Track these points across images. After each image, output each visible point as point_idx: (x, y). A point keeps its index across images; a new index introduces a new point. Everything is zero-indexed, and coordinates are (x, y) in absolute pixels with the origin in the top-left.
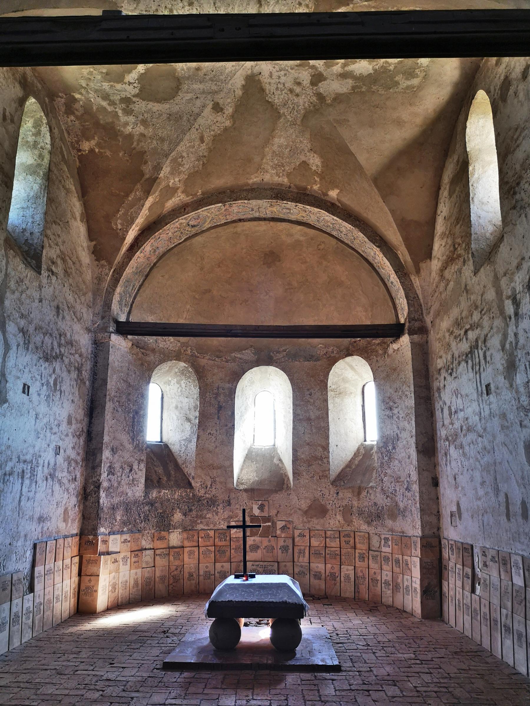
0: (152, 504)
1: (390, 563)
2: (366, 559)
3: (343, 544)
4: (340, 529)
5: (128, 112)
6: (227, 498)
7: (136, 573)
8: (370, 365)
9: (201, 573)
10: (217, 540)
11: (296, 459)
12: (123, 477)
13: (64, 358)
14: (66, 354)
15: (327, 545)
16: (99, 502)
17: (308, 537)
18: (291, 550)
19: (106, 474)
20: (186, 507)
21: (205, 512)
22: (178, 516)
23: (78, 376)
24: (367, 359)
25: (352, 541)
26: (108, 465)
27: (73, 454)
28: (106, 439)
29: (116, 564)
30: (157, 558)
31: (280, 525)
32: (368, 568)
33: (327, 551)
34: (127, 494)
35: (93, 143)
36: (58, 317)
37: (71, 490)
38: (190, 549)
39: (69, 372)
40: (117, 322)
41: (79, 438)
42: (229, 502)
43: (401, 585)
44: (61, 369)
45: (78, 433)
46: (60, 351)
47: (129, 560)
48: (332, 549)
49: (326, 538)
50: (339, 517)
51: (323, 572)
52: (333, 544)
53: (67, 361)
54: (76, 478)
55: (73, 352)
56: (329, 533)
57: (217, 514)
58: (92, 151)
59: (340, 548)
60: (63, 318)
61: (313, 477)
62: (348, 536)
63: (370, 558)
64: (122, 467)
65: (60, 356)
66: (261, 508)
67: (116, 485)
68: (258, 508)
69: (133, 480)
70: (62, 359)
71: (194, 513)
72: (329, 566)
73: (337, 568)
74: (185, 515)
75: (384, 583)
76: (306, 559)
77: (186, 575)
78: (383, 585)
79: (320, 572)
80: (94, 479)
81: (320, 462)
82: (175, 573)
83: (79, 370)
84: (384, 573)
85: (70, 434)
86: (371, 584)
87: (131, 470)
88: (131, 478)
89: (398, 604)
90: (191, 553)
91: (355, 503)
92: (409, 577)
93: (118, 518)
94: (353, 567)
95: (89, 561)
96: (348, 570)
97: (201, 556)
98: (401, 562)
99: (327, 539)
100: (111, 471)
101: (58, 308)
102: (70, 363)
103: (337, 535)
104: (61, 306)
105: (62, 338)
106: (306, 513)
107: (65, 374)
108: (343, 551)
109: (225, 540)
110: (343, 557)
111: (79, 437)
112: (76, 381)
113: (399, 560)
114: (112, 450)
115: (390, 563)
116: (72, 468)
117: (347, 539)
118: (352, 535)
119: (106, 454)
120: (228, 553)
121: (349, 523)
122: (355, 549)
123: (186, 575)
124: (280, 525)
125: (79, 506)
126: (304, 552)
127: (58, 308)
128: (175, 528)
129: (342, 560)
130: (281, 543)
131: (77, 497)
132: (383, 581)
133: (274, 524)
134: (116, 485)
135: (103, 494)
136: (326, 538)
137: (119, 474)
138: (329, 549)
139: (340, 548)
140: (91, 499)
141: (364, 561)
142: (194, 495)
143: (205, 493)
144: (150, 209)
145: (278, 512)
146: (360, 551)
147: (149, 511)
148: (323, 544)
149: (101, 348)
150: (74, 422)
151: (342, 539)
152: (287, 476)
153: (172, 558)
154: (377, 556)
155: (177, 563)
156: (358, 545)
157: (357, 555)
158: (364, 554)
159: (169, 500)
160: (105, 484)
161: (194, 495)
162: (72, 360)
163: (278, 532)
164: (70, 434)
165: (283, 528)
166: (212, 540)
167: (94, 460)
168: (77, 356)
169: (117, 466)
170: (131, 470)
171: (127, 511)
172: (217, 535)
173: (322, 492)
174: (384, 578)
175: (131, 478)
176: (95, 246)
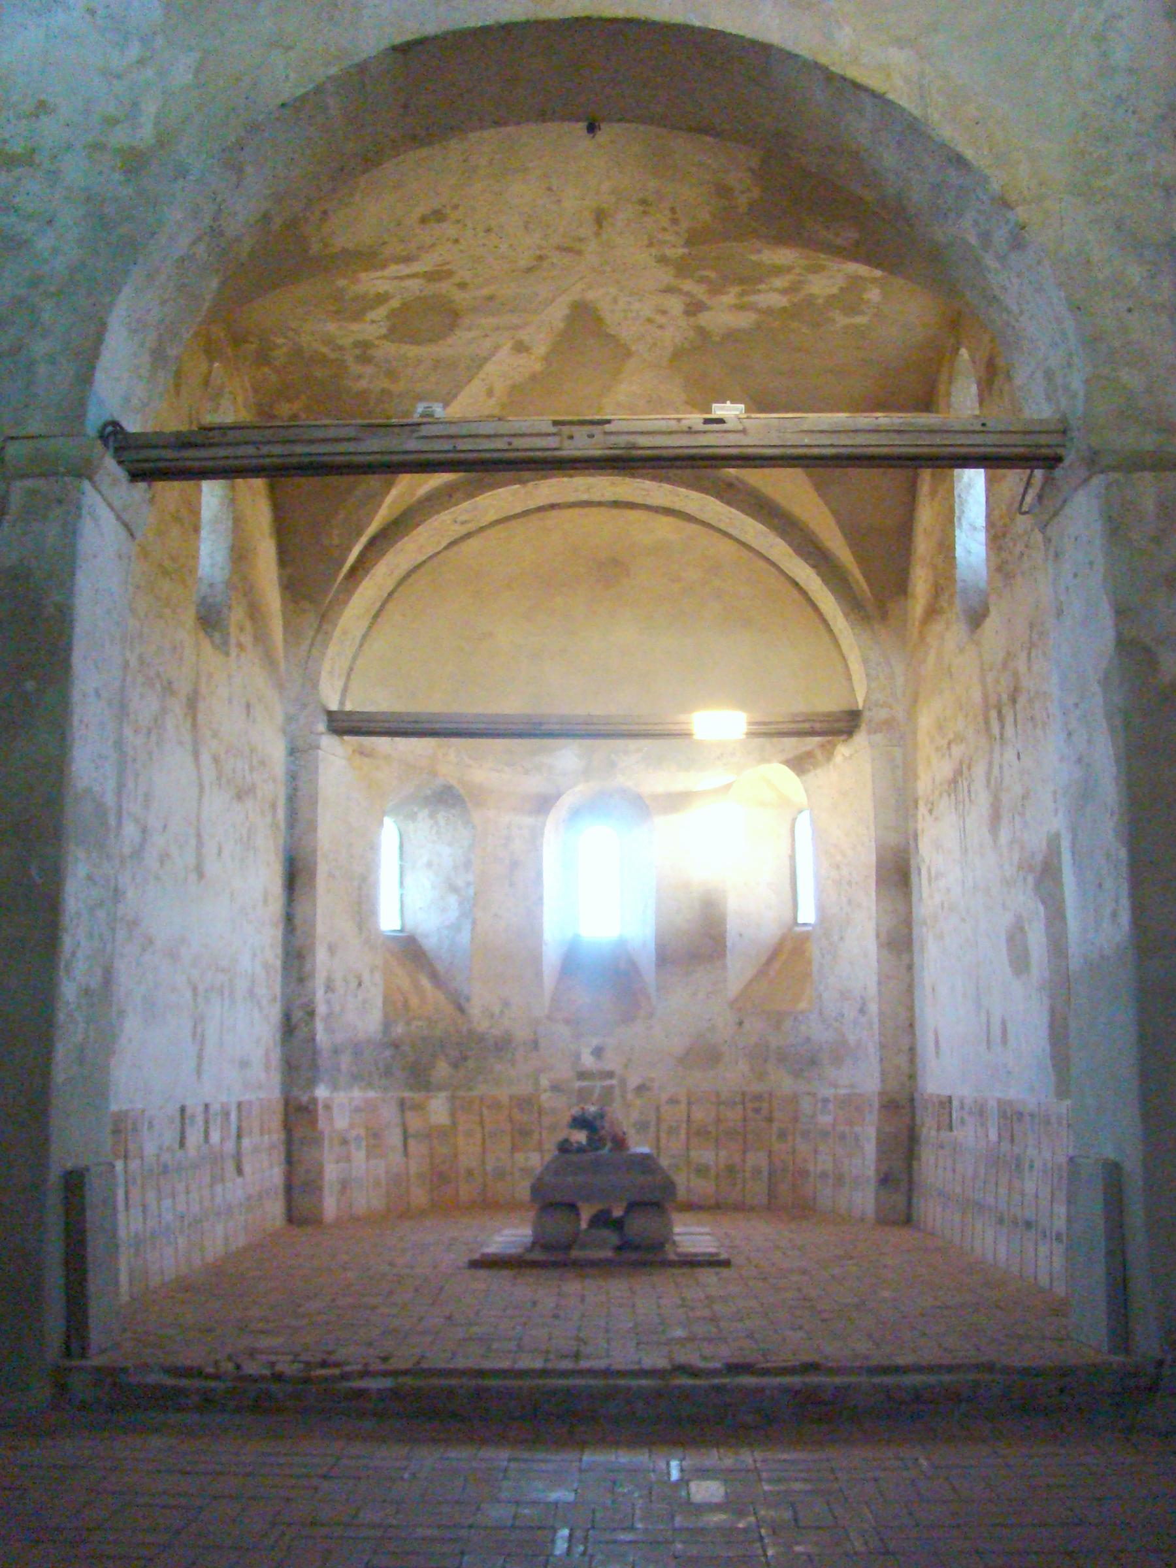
0: (396, 1046)
9: (489, 1168)
18: (652, 1129)
22: (442, 1069)
25: (765, 1105)
30: (411, 1141)
40: (330, 714)
64: (345, 980)
68: (592, 1053)
71: (471, 1064)
74: (455, 1065)
93: (344, 1067)
96: (759, 1158)
110: (750, 1137)
120: (536, 1136)
128: (440, 1088)
144: (389, 507)
149: (303, 763)
151: (749, 1105)
155: (443, 1150)
170: (360, 984)
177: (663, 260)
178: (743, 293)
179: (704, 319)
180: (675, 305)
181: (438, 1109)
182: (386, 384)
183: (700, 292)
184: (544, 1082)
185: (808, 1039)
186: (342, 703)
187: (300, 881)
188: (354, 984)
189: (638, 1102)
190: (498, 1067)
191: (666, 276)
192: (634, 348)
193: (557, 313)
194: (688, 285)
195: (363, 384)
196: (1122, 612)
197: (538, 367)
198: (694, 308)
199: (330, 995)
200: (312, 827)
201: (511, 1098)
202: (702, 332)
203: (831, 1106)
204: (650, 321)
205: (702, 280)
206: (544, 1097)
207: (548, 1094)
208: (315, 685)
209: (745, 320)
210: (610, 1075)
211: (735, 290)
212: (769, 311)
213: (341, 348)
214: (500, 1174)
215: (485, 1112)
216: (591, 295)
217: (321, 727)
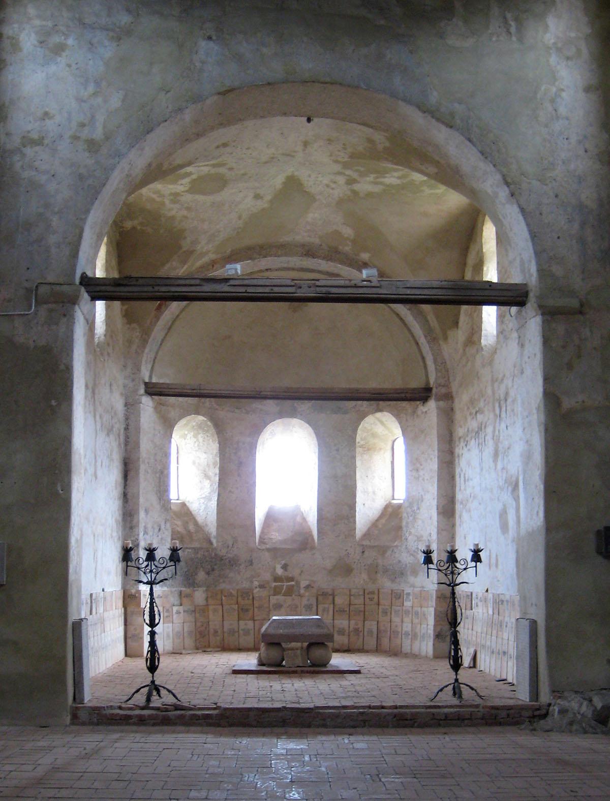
1: (410, 616)
2: (389, 614)
3: (367, 600)
5: (173, 202)
8: (400, 423)
10: (240, 599)
11: (321, 518)
15: (352, 603)
20: (209, 567)
22: (201, 575)
24: (397, 416)
25: (376, 597)
31: (303, 584)
32: (391, 622)
33: (351, 608)
35: (136, 222)
38: (214, 607)
42: (252, 561)
43: (419, 634)
48: (356, 606)
50: (364, 576)
51: (347, 628)
52: (356, 601)
56: (353, 591)
57: (239, 573)
58: (134, 228)
59: (364, 604)
61: (339, 536)
62: (373, 593)
63: (393, 613)
66: (285, 567)
68: (282, 568)
69: (162, 539)
71: (217, 572)
72: (352, 622)
73: (360, 625)
74: (208, 573)
75: (404, 634)
76: (331, 616)
78: (403, 636)
79: (343, 629)
81: (346, 522)
84: (405, 625)
86: (392, 636)
87: (160, 530)
88: (160, 537)
89: (415, 650)
90: (215, 610)
91: (380, 561)
92: (425, 626)
94: (376, 623)
97: (225, 615)
98: (419, 613)
99: (352, 597)
103: (361, 593)
106: (330, 571)
108: (367, 608)
109: (248, 599)
110: (367, 613)
113: (418, 612)
115: (410, 616)
117: (371, 596)
118: (376, 592)
120: (251, 613)
121: (374, 580)
122: (379, 605)
124: (303, 584)
126: (328, 611)
129: (366, 616)
130: (305, 601)
132: (403, 633)
133: (298, 583)
136: (350, 595)
138: (353, 606)
139: (364, 604)
145: (302, 572)
146: (384, 607)
148: (347, 602)
149: (132, 411)
151: (367, 596)
152: (311, 536)
154: (399, 611)
156: (382, 602)
157: (380, 610)
158: (387, 609)
159: (192, 559)
163: (302, 591)
165: (308, 587)
170: (160, 530)
173: (347, 551)
174: (405, 629)
175: (160, 537)
176: (126, 310)
177: (336, 162)
178: (377, 178)
179: (356, 187)
180: (341, 180)
181: (200, 596)
182: (185, 213)
183: (355, 175)
184: (256, 583)
185: (400, 561)
186: (151, 377)
187: (131, 474)
188: (156, 530)
189: (307, 594)
190: (231, 575)
191: (337, 168)
192: (317, 197)
193: (279, 181)
194: (348, 172)
195: (173, 213)
196: (546, 379)
197: (266, 205)
198: (351, 181)
199: (146, 536)
200: (137, 445)
201: (238, 590)
202: (355, 193)
203: (411, 598)
204: (328, 186)
205: (357, 171)
206: (255, 591)
207: (258, 589)
208: (139, 370)
209: (377, 189)
210: (292, 579)
211: (373, 176)
212: (390, 186)
213: (164, 196)
214: (232, 632)
215: (224, 598)
216: (296, 173)
217: (142, 391)
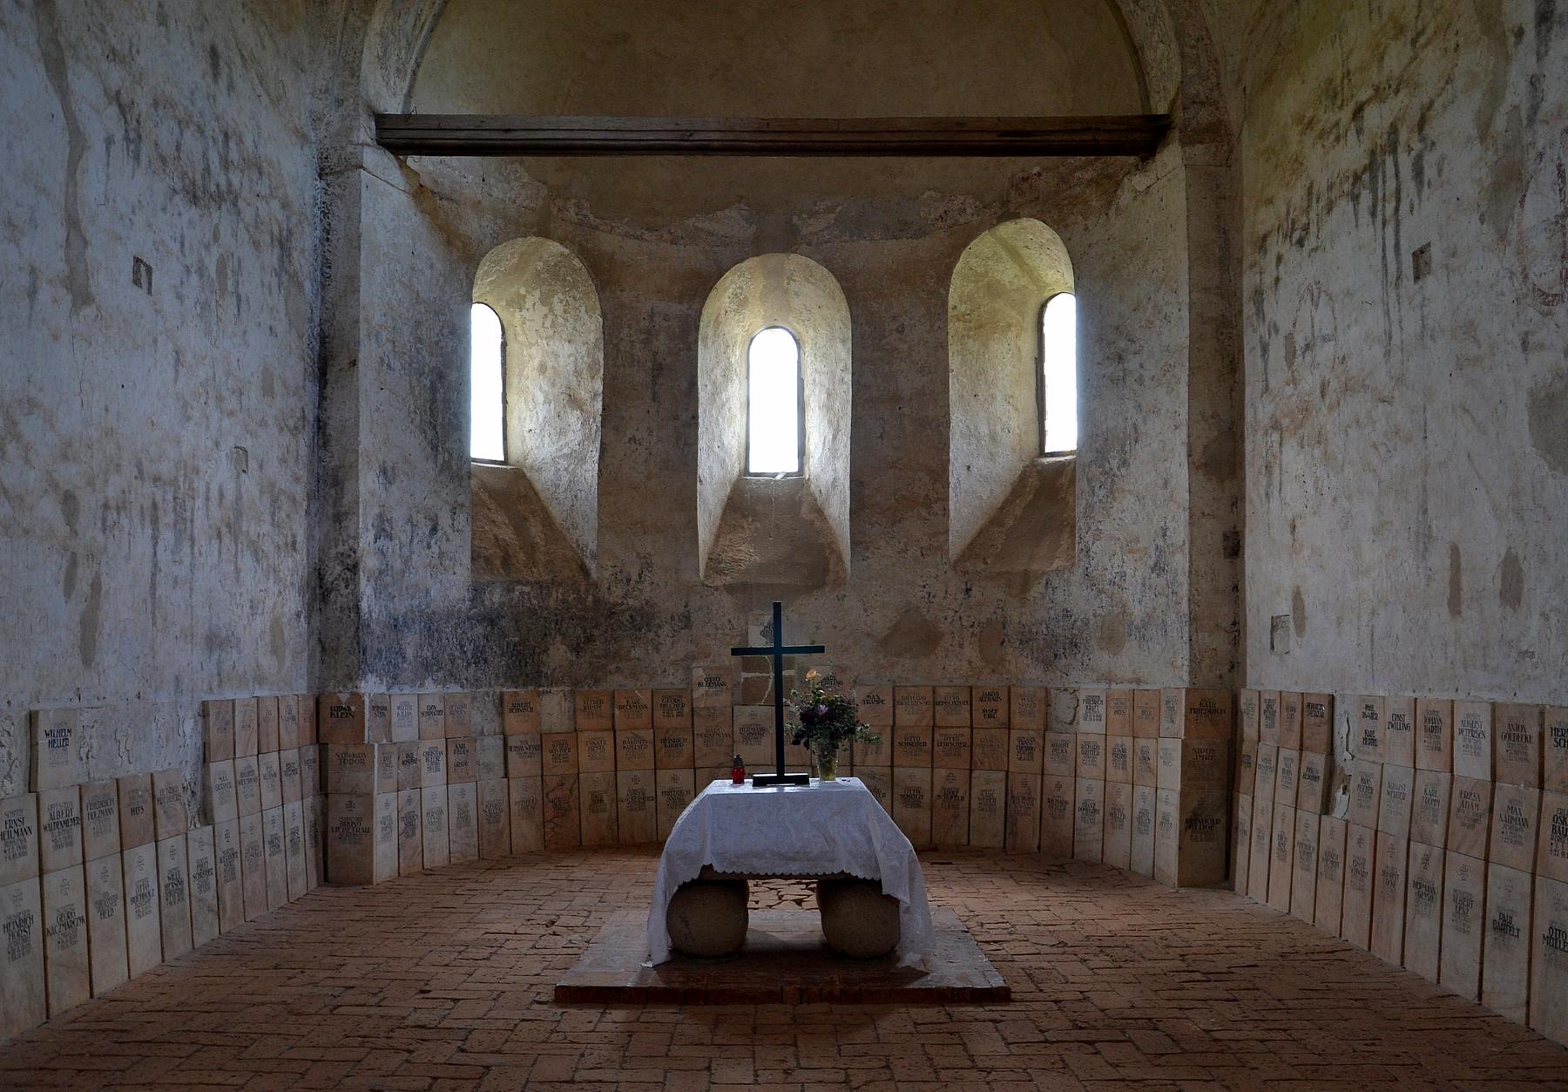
2: (1037, 754)
3: (978, 716)
4: (972, 682)
6: (683, 610)
7: (463, 793)
12: (416, 547)
13: (241, 204)
14: (245, 194)
16: (357, 607)
17: (889, 703)
19: (371, 536)
21: (626, 643)
22: (558, 654)
23: (281, 261)
26: (376, 511)
27: (283, 481)
28: (366, 441)
29: (413, 766)
34: (427, 592)
36: (216, 82)
37: (285, 572)
39: (256, 245)
41: (294, 436)
44: (235, 235)
45: (291, 423)
46: (230, 184)
47: (443, 759)
49: (935, 703)
53: (248, 213)
54: (294, 543)
55: (265, 191)
56: (942, 692)
57: (657, 649)
60: (231, 87)
62: (992, 696)
64: (410, 520)
65: (225, 197)
67: (398, 565)
69: (441, 555)
70: (235, 205)
74: (576, 649)
77: (586, 799)
80: (341, 549)
82: (559, 793)
83: (284, 244)
85: (271, 422)
87: (434, 530)
88: (435, 549)
93: (410, 653)
95: (343, 760)
96: (989, 782)
100: (383, 530)
101: (214, 53)
102: (258, 223)
103: (964, 697)
104: (221, 48)
105: (232, 145)
107: (245, 251)
108: (978, 735)
109: (680, 714)
110: (978, 751)
111: (295, 431)
112: (278, 275)
114: (384, 471)
116: (283, 514)
117: (990, 705)
118: (1003, 695)
119: (367, 483)
123: (586, 799)
125: (309, 617)
127: (214, 53)
128: (553, 682)
131: (301, 592)
134: (398, 565)
135: (366, 588)
136: (935, 703)
137: (405, 539)
140: (339, 598)
141: (1031, 757)
142: (597, 601)
143: (626, 596)
146: (1024, 734)
147: (486, 637)
150: (278, 388)
153: (548, 756)
156: (1017, 720)
157: (1014, 743)
159: (532, 612)
160: (370, 562)
161: (597, 601)
162: (263, 214)
164: (271, 422)
166: (646, 714)
167: (338, 499)
168: (275, 204)
169: (398, 516)
170: (434, 530)
171: (431, 637)
172: (659, 701)
175: (435, 549)
